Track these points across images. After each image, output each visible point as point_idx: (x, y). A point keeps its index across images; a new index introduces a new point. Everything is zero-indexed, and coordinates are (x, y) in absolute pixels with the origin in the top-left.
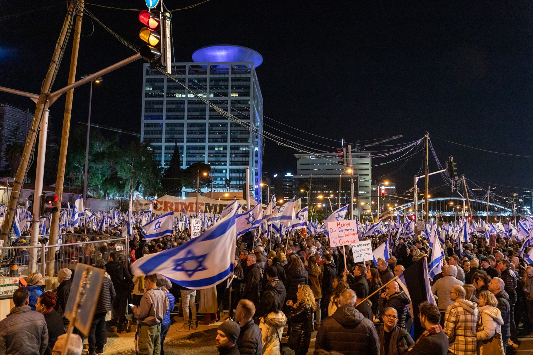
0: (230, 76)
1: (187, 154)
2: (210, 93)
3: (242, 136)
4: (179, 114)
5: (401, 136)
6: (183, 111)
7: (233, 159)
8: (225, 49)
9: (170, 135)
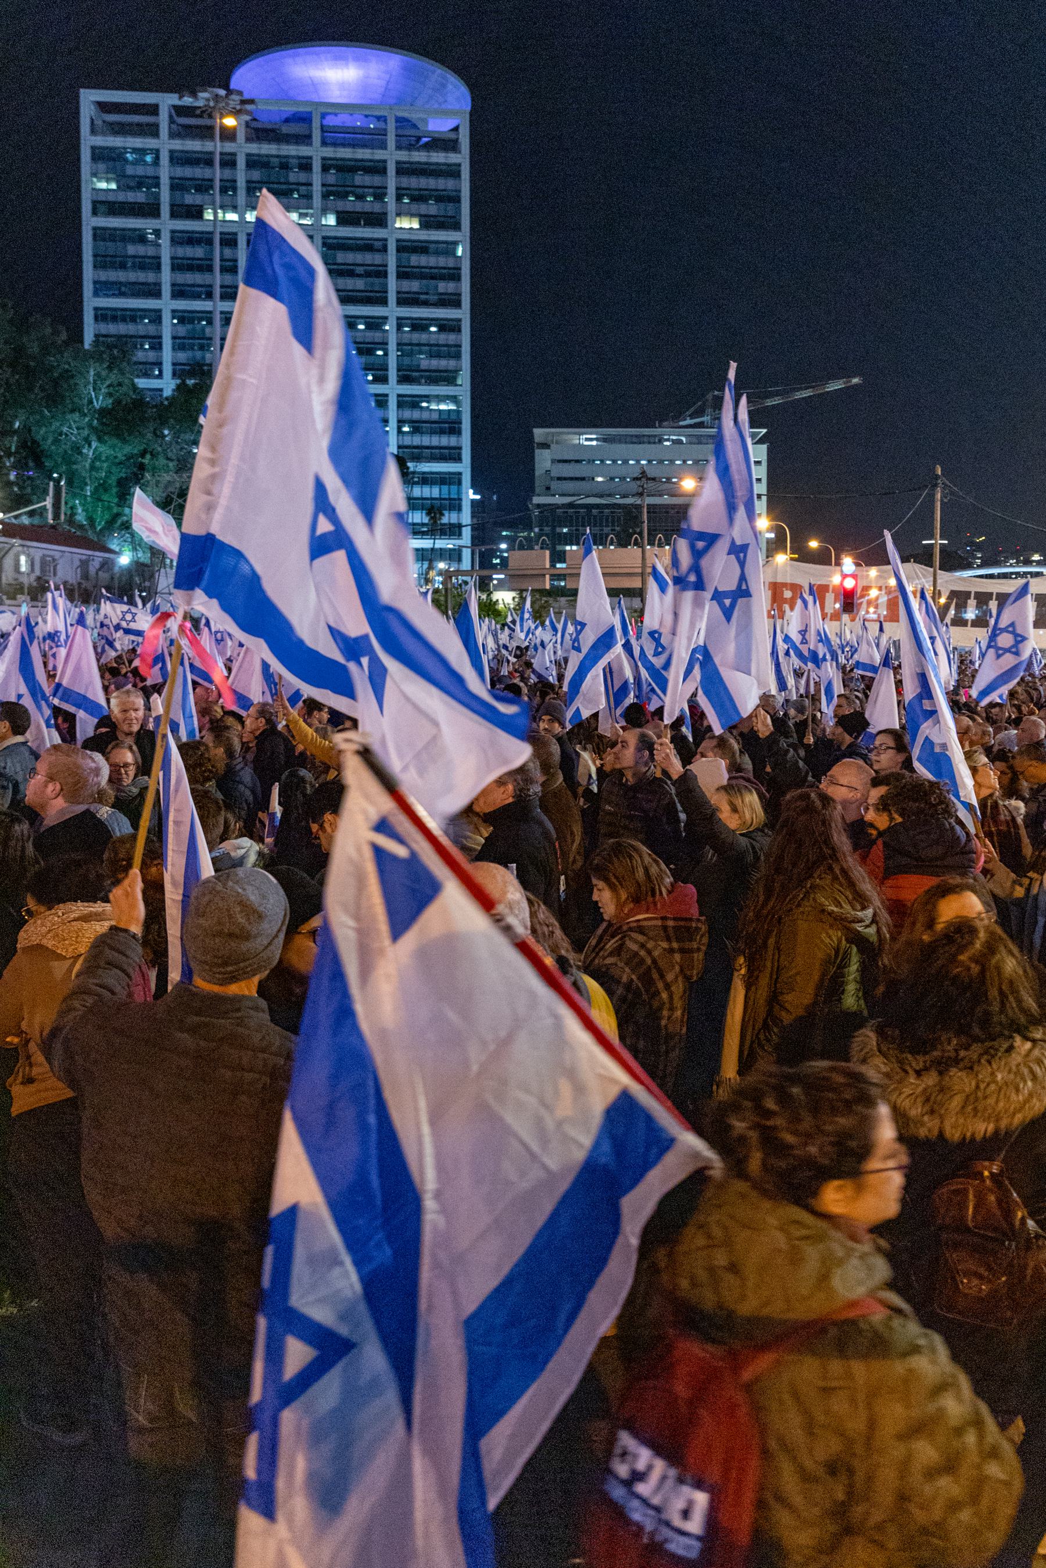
0: (391, 155)
2: (324, 211)
3: (435, 363)
5: (855, 381)
7: (407, 441)
9: (190, 353)
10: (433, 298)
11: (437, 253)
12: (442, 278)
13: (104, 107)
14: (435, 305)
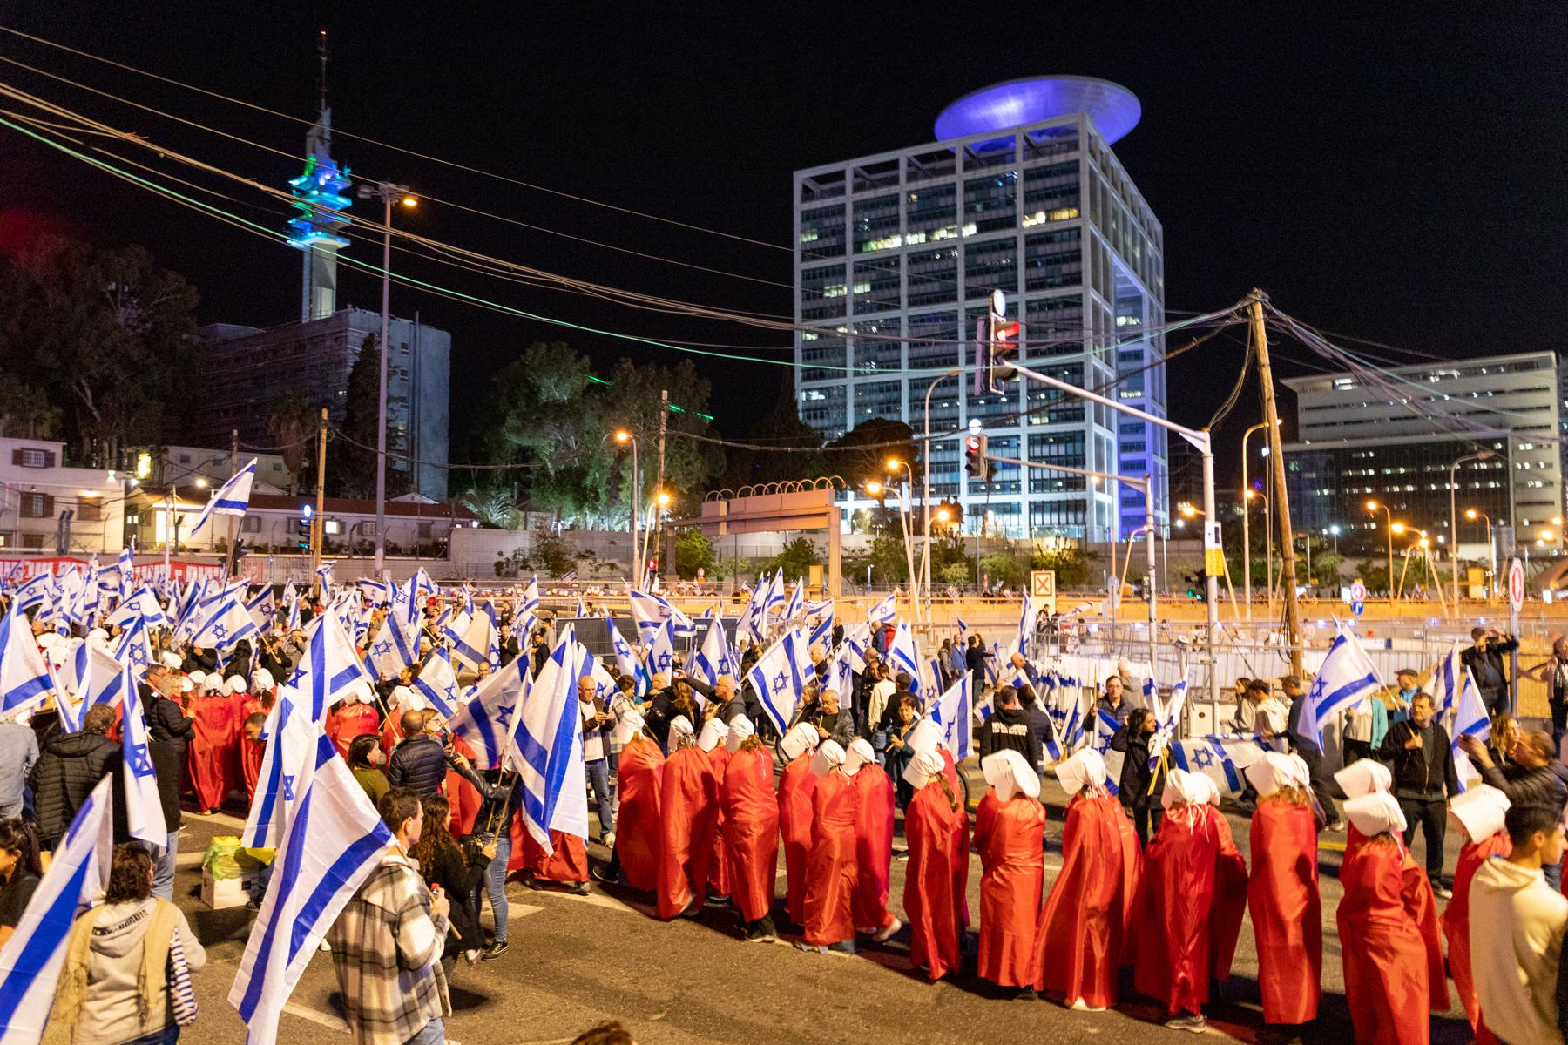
1: (911, 401)
2: (966, 223)
6: (897, 285)
8: (1014, 93)
10: (1058, 280)
11: (1062, 240)
12: (1065, 260)
13: (820, 179)
14: (1060, 285)
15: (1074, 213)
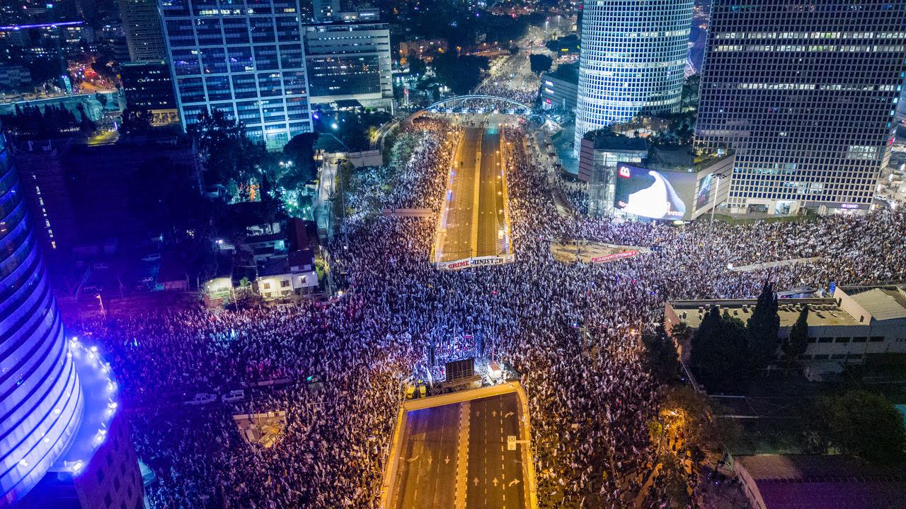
4: (215, 36)
15: (293, 10)
